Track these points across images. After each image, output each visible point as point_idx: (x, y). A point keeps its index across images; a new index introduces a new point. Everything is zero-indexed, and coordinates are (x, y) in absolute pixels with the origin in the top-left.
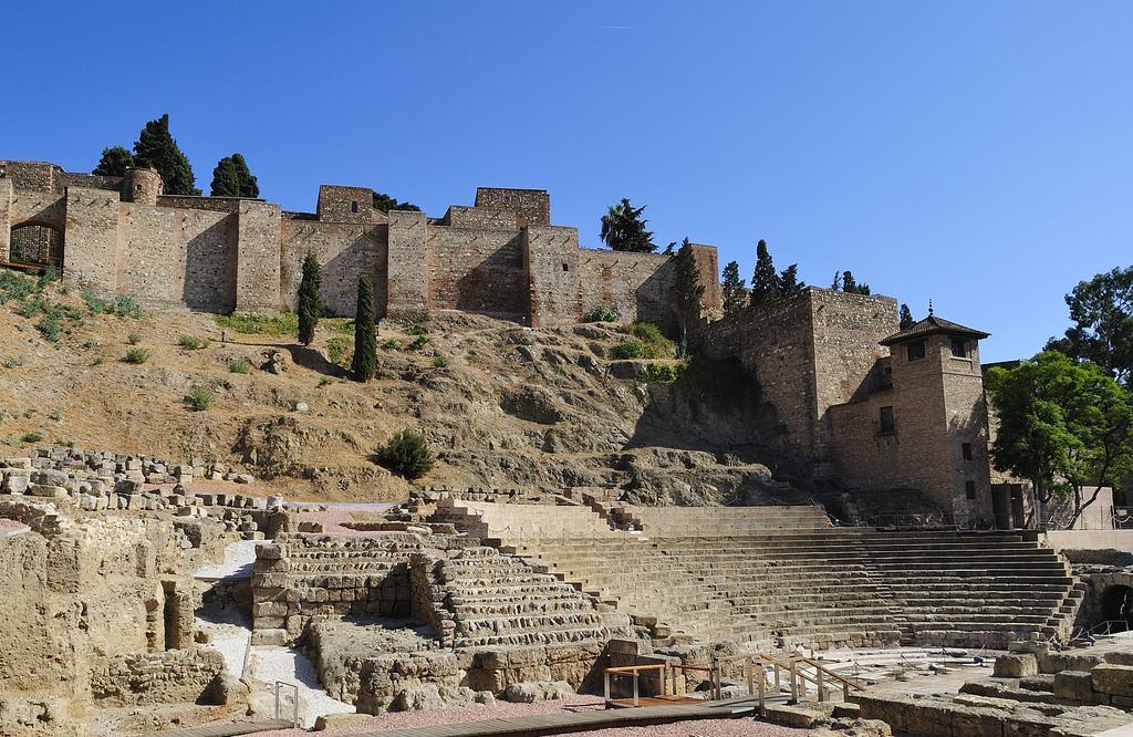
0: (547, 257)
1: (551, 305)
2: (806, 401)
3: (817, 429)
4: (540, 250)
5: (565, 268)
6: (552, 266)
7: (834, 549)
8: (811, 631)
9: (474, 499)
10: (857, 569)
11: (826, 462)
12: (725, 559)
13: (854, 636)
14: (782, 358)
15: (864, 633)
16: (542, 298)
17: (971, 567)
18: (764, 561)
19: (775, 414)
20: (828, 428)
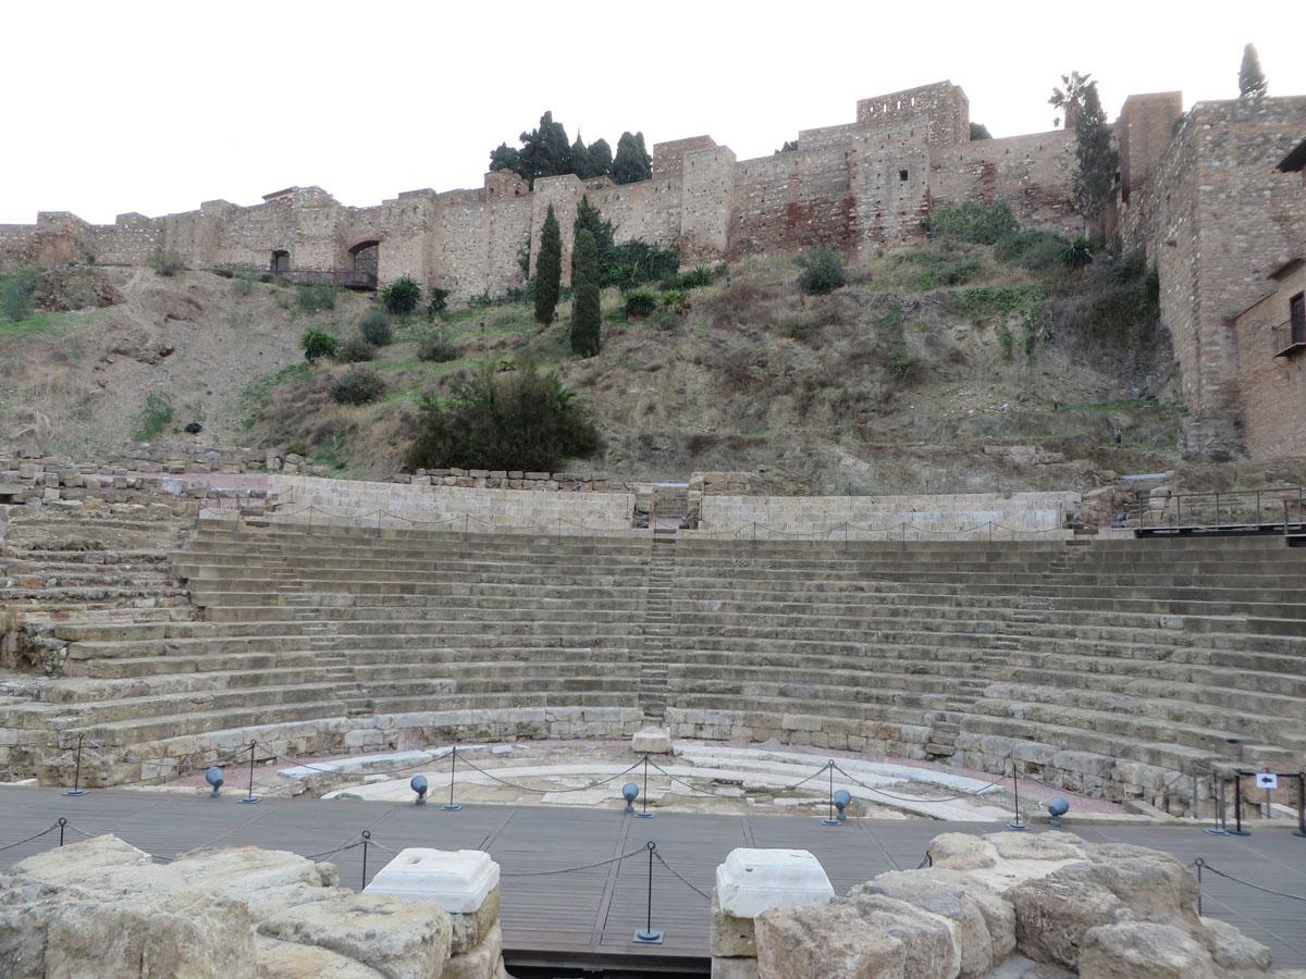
0: (877, 167)
1: (878, 234)
2: (1195, 312)
3: (1203, 359)
4: (866, 160)
5: (904, 175)
6: (882, 181)
7: (1005, 566)
8: (747, 705)
9: (510, 486)
10: (1006, 604)
11: (1216, 417)
12: (778, 577)
13: (833, 726)
14: (1172, 244)
15: (853, 723)
16: (867, 224)
17: (1233, 610)
18: (844, 583)
19: (1170, 347)
20: (1230, 356)
